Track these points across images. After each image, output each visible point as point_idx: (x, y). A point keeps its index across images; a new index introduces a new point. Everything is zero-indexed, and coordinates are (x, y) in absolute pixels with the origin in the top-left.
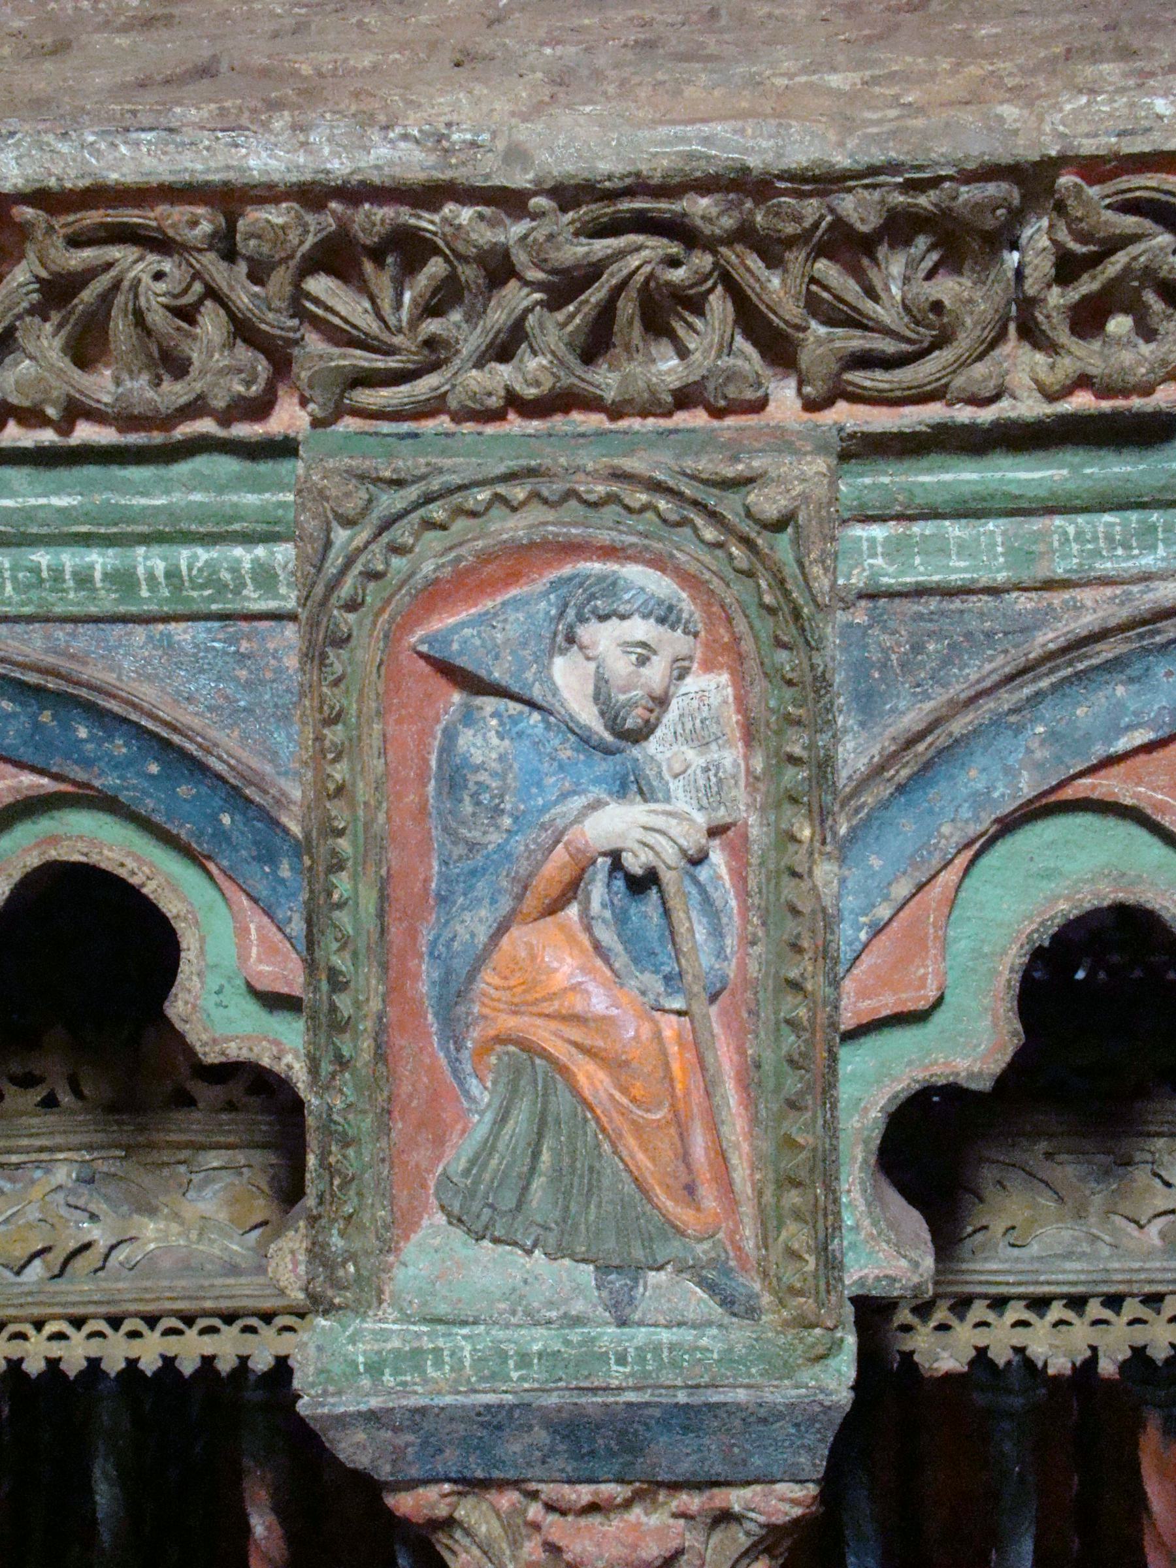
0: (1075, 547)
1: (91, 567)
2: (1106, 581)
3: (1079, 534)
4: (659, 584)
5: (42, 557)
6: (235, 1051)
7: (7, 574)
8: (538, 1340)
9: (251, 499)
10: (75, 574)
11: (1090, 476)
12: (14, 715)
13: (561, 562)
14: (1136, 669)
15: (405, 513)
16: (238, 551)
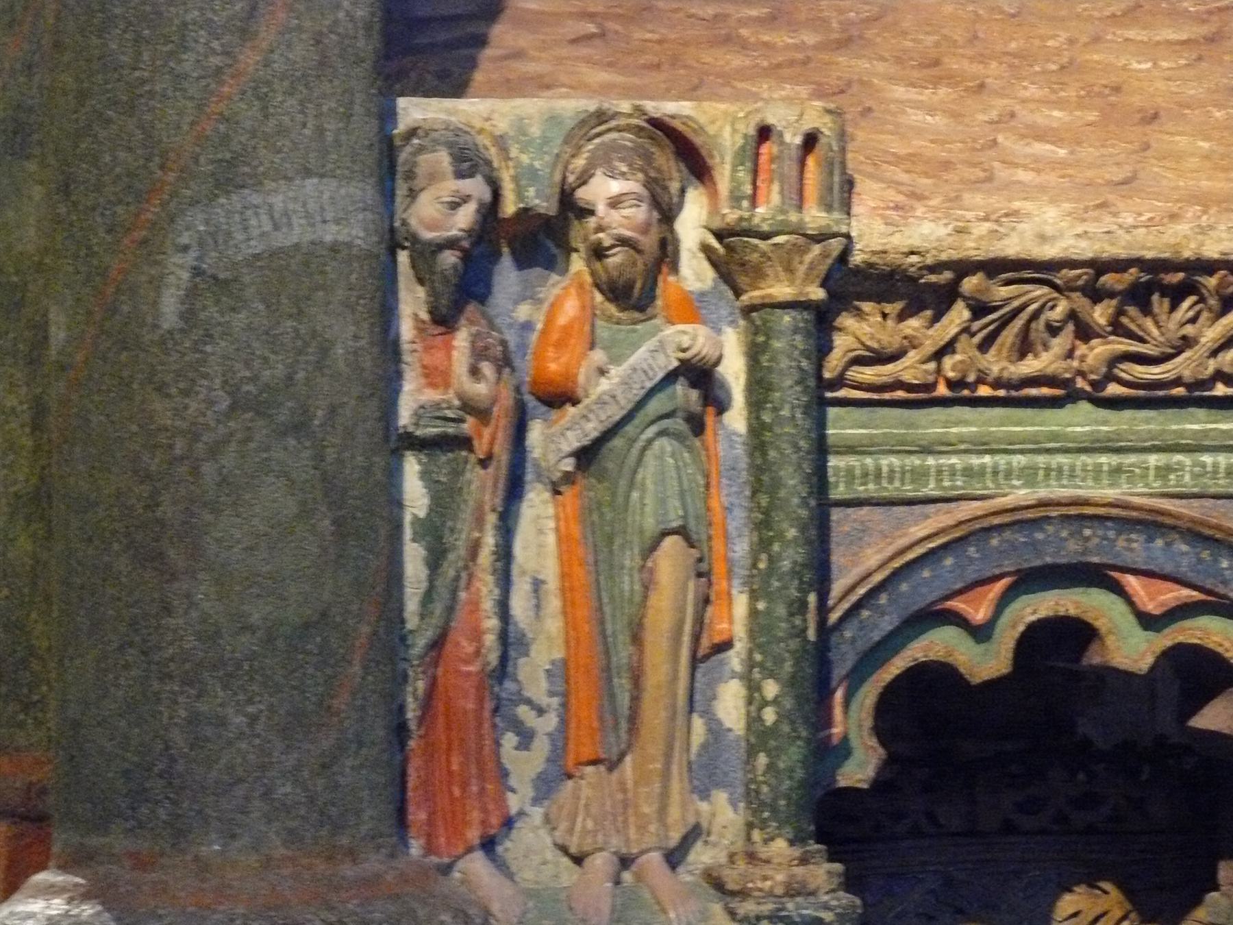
5: (1207, 459)
12: (1186, 554)
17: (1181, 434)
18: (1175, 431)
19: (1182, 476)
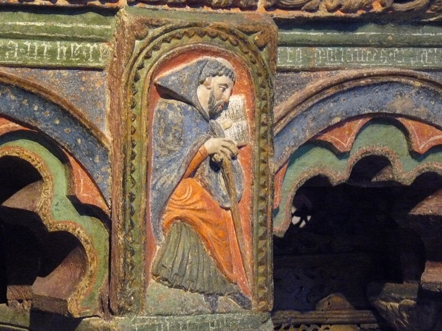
0: (321, 57)
1: (43, 48)
2: (327, 69)
3: (322, 53)
4: (228, 64)
5: (28, 43)
6: (61, 227)
7: (16, 49)
8: (189, 319)
9: (97, 27)
10: (38, 50)
11: (328, 35)
12: (15, 101)
13: (199, 55)
14: (336, 98)
15: (158, 36)
16: (88, 45)
17: (14, 27)
18: (10, 26)
19: (14, 54)
